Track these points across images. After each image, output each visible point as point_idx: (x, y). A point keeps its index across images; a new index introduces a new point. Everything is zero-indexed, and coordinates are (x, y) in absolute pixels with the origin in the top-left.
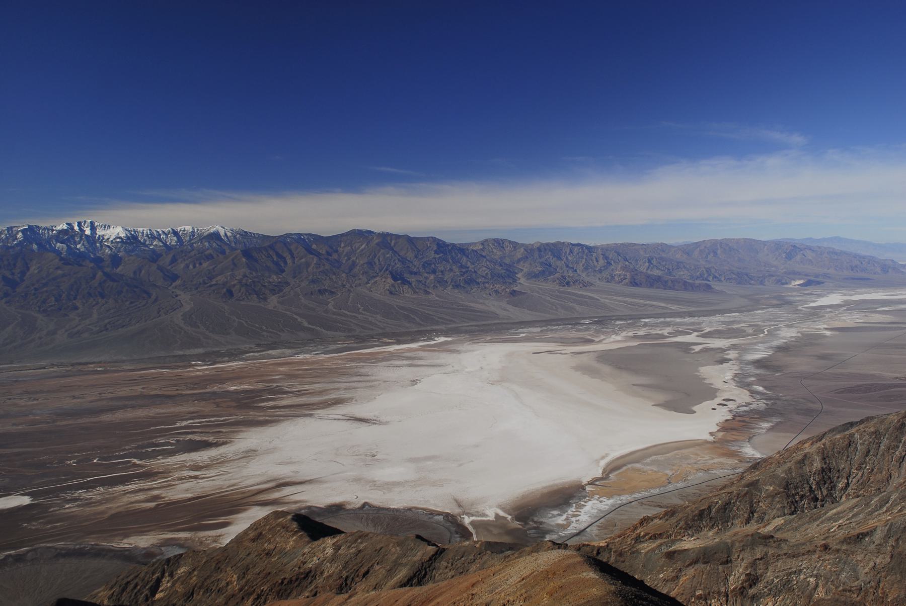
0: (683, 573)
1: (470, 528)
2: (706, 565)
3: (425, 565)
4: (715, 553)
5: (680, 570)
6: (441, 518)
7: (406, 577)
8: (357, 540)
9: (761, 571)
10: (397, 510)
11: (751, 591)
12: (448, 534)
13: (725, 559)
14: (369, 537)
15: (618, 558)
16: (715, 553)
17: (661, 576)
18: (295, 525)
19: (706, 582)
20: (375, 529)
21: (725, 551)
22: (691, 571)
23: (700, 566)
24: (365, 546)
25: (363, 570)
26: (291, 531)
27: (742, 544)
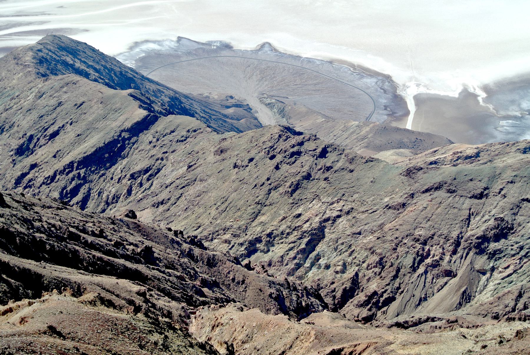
0: (415, 201)
1: (411, 106)
2: (449, 195)
3: (123, 134)
4: (471, 180)
5: (412, 196)
6: (370, 81)
7: (92, 147)
8: (62, 87)
9: (523, 218)
10: (309, 60)
11: (493, 246)
12: (371, 107)
13: (479, 191)
14: (77, 85)
15: (347, 165)
16: (471, 180)
17: (386, 200)
18: (28, 58)
19: (437, 220)
20: (258, 85)
21: (486, 179)
22: (423, 200)
23: (442, 194)
24: (68, 97)
25: (51, 131)
26: (21, 64)
27: (515, 173)
